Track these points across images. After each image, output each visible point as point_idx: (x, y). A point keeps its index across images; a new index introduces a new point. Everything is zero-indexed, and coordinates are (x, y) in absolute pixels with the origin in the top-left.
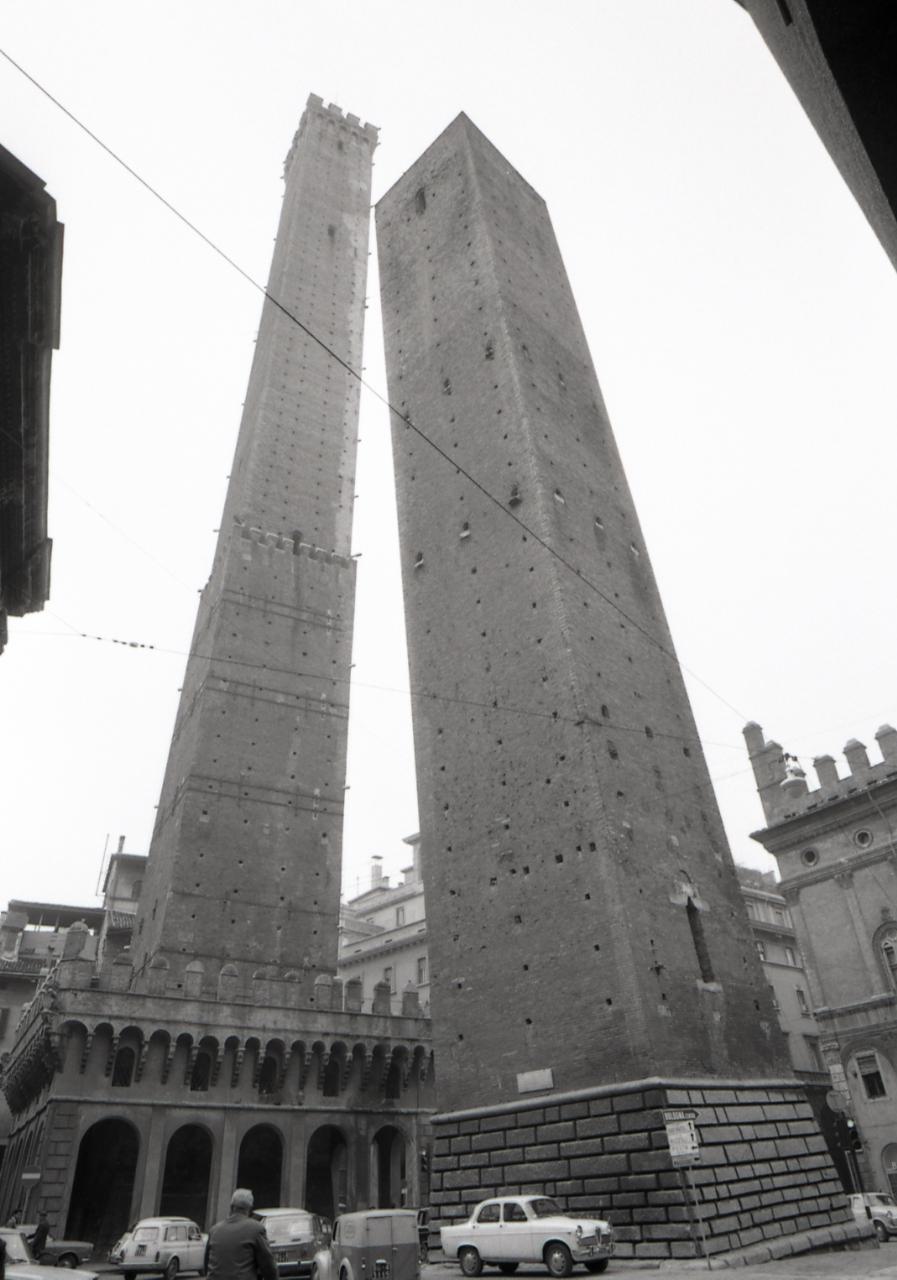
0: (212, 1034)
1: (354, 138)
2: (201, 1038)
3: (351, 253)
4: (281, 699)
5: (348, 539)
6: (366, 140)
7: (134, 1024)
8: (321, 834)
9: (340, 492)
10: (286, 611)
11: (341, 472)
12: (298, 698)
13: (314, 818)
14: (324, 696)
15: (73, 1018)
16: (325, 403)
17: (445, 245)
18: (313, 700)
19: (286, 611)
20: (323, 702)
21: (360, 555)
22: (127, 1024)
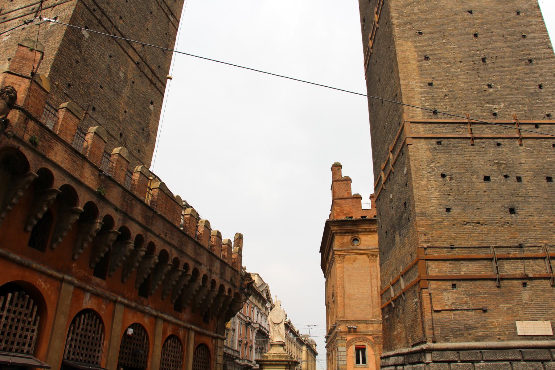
0: (127, 225)
2: (120, 226)
7: (73, 184)
8: (150, 101)
15: (15, 144)
22: (67, 181)
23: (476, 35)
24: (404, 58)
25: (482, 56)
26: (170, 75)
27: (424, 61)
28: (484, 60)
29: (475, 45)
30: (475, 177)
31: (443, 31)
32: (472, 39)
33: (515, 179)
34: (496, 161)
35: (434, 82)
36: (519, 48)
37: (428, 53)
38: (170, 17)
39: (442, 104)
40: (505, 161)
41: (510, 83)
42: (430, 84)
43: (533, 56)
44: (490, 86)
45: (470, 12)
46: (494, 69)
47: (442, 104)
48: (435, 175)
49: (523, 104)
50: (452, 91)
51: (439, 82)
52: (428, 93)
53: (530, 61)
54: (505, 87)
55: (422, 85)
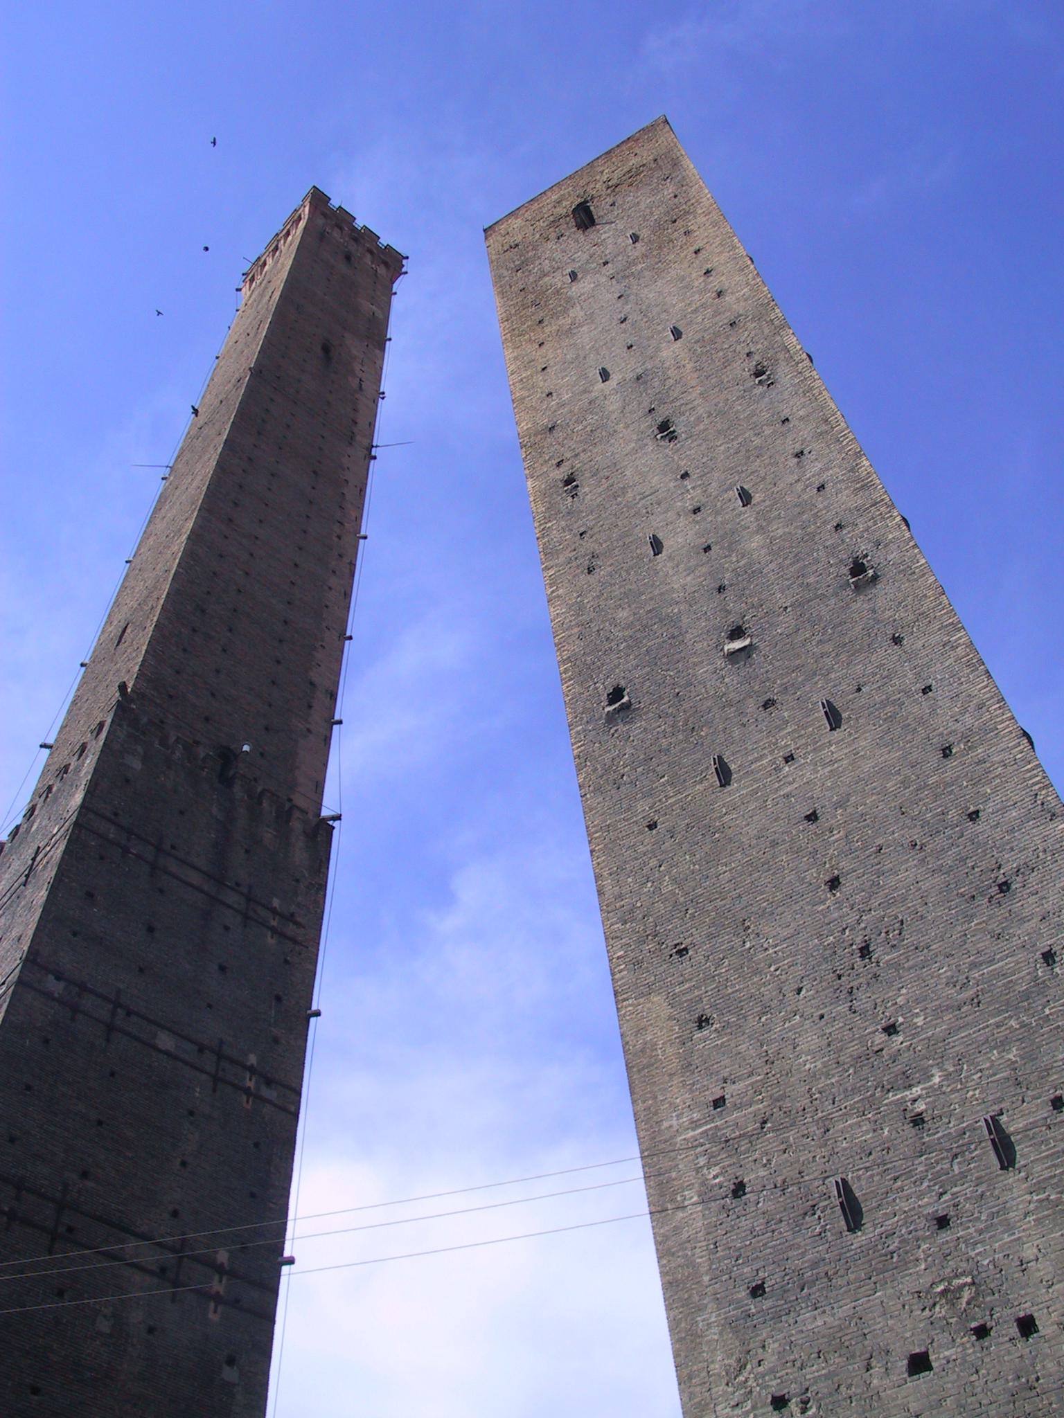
1: (369, 256)
3: (354, 383)
4: (165, 1041)
5: (319, 787)
6: (386, 264)
9: (310, 707)
10: (195, 878)
11: (314, 675)
12: (201, 1049)
13: (211, 1316)
14: (252, 1059)
16: (296, 565)
17: (645, 256)
18: (232, 1061)
19: (195, 878)
20: (252, 1070)
21: (338, 818)
23: (834, 883)
24: (643, 1050)
25: (859, 940)
26: (287, 1253)
27: (698, 1035)
28: (865, 951)
29: (835, 915)
30: (877, 1369)
31: (744, 915)
32: (823, 902)
33: (1014, 1331)
34: (941, 1287)
35: (731, 1090)
36: (963, 860)
37: (705, 1008)
38: (266, 1092)
39: (757, 1155)
40: (970, 1273)
41: (952, 991)
42: (719, 1103)
43: (1010, 862)
44: (891, 1030)
45: (812, 817)
46: (897, 966)
47: (757, 1155)
48: (754, 1408)
49: (1003, 1045)
50: (783, 1097)
51: (740, 1085)
52: (712, 1137)
53: (1004, 887)
54: (940, 1011)
55: (696, 1116)
